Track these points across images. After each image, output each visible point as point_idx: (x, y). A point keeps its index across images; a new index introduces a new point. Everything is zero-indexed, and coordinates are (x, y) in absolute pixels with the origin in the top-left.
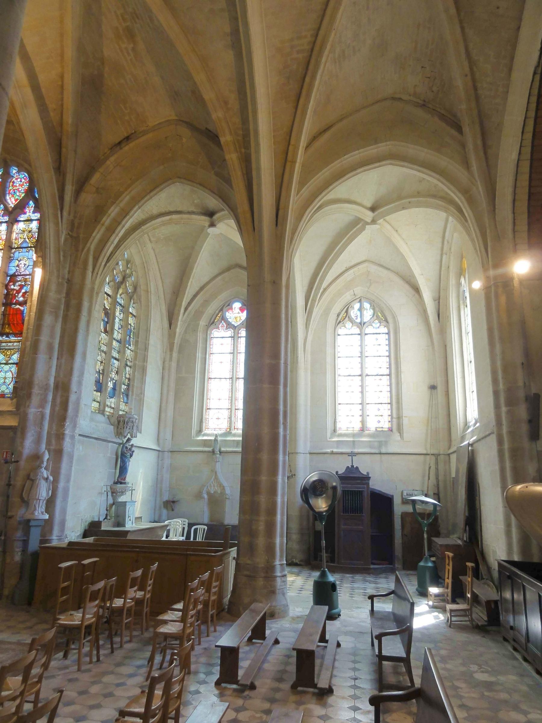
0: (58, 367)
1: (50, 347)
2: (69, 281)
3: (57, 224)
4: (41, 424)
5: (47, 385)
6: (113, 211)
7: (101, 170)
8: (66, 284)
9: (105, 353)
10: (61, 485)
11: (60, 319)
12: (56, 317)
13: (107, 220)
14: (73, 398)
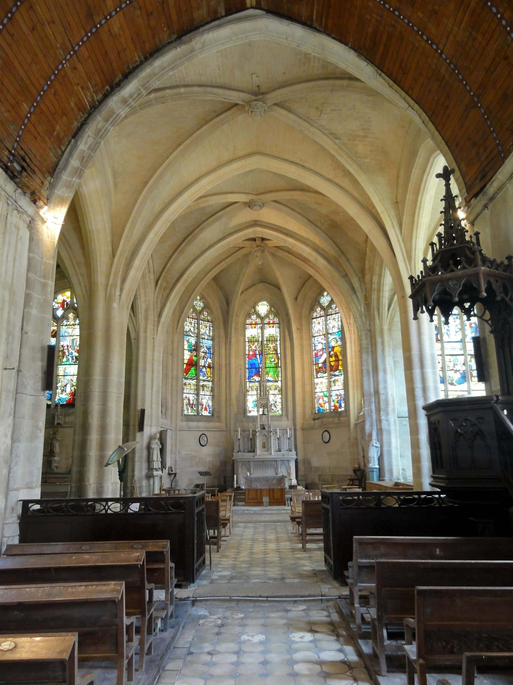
0: (374, 381)
1: (368, 371)
2: (370, 331)
3: (355, 303)
4: (371, 416)
5: (371, 393)
6: (375, 279)
7: (367, 258)
8: (369, 333)
9: (440, 355)
10: (385, 449)
11: (370, 354)
12: (368, 354)
13: (375, 286)
14: (382, 397)
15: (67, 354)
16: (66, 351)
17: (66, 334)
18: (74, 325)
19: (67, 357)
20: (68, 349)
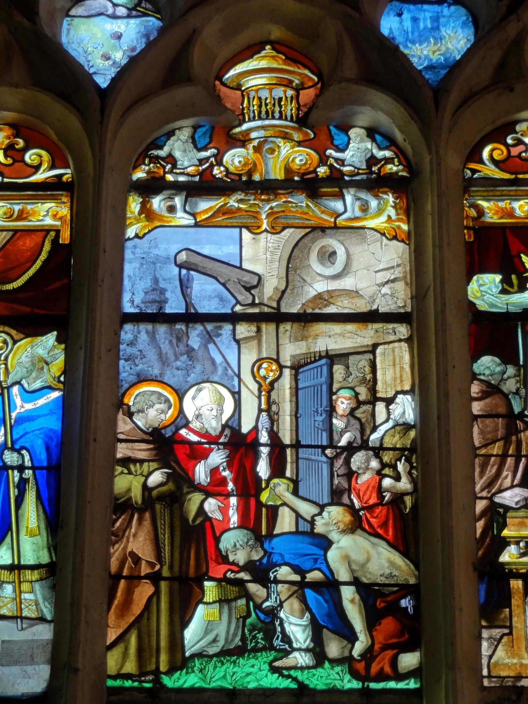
15: (235, 543)
16: (224, 511)
17: (207, 295)
18: (310, 185)
19: (234, 590)
20: (249, 487)
